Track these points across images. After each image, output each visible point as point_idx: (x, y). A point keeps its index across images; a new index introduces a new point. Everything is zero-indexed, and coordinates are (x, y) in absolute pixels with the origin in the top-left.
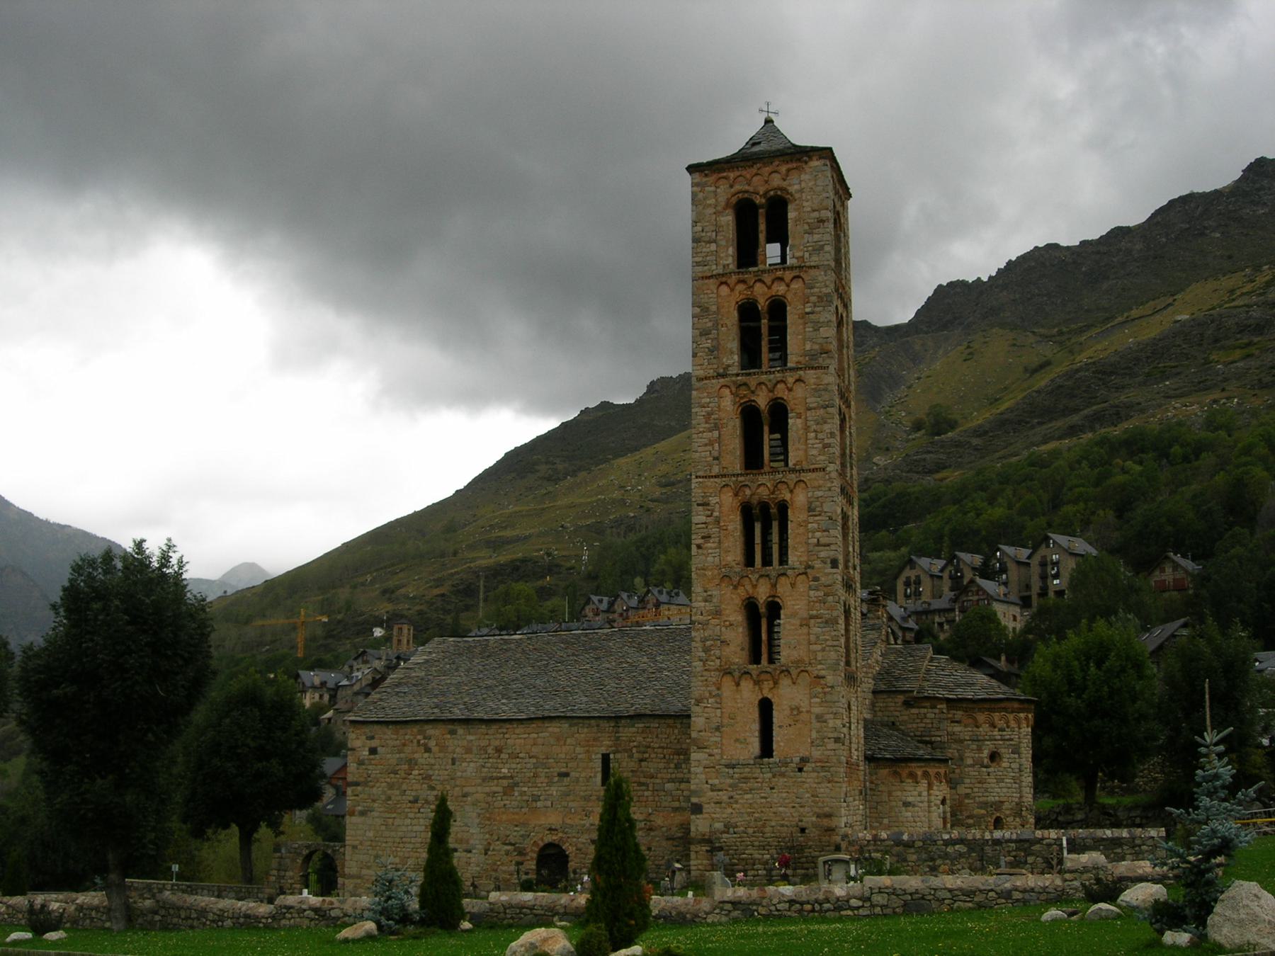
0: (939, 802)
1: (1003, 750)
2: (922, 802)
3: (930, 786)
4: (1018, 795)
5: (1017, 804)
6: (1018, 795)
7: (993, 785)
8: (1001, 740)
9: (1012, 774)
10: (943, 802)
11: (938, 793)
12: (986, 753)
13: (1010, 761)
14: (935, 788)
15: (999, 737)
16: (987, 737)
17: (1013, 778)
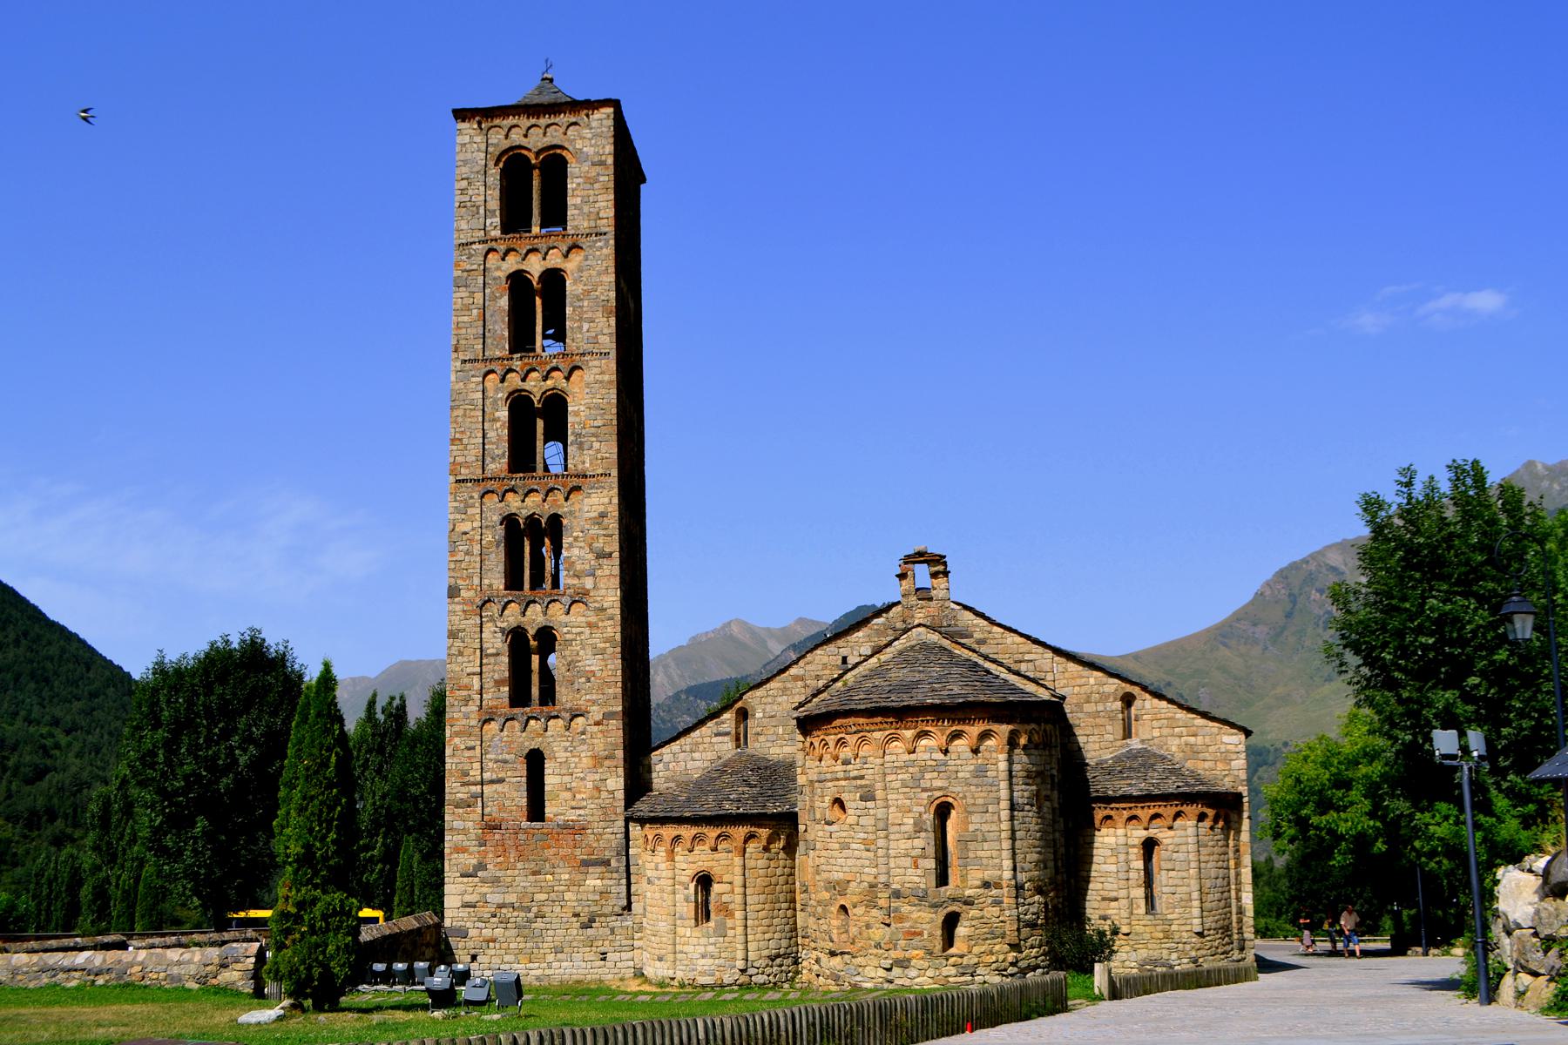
0: (686, 880)
1: (844, 797)
2: (659, 879)
3: (671, 854)
4: (874, 871)
5: (872, 886)
6: (874, 871)
7: (835, 854)
8: (846, 779)
9: (862, 835)
10: (704, 881)
11: (684, 866)
12: (827, 799)
13: (859, 813)
14: (677, 858)
15: (841, 775)
16: (829, 776)
17: (864, 841)
